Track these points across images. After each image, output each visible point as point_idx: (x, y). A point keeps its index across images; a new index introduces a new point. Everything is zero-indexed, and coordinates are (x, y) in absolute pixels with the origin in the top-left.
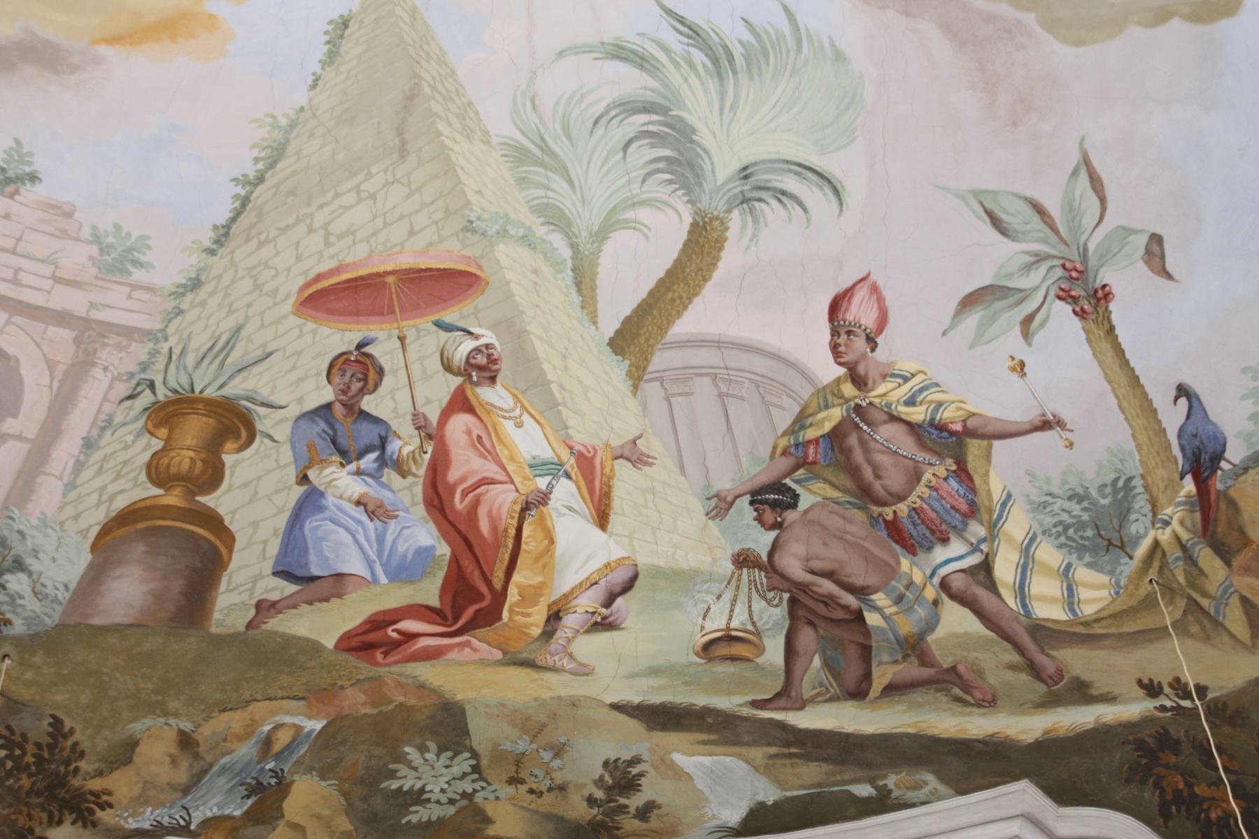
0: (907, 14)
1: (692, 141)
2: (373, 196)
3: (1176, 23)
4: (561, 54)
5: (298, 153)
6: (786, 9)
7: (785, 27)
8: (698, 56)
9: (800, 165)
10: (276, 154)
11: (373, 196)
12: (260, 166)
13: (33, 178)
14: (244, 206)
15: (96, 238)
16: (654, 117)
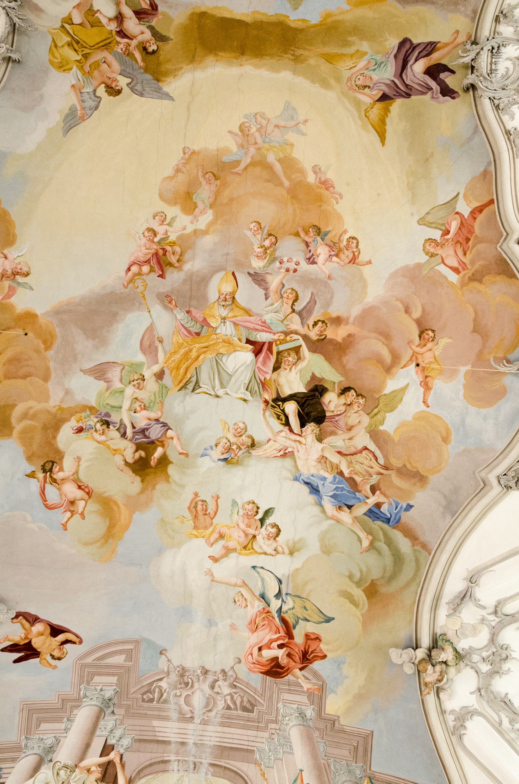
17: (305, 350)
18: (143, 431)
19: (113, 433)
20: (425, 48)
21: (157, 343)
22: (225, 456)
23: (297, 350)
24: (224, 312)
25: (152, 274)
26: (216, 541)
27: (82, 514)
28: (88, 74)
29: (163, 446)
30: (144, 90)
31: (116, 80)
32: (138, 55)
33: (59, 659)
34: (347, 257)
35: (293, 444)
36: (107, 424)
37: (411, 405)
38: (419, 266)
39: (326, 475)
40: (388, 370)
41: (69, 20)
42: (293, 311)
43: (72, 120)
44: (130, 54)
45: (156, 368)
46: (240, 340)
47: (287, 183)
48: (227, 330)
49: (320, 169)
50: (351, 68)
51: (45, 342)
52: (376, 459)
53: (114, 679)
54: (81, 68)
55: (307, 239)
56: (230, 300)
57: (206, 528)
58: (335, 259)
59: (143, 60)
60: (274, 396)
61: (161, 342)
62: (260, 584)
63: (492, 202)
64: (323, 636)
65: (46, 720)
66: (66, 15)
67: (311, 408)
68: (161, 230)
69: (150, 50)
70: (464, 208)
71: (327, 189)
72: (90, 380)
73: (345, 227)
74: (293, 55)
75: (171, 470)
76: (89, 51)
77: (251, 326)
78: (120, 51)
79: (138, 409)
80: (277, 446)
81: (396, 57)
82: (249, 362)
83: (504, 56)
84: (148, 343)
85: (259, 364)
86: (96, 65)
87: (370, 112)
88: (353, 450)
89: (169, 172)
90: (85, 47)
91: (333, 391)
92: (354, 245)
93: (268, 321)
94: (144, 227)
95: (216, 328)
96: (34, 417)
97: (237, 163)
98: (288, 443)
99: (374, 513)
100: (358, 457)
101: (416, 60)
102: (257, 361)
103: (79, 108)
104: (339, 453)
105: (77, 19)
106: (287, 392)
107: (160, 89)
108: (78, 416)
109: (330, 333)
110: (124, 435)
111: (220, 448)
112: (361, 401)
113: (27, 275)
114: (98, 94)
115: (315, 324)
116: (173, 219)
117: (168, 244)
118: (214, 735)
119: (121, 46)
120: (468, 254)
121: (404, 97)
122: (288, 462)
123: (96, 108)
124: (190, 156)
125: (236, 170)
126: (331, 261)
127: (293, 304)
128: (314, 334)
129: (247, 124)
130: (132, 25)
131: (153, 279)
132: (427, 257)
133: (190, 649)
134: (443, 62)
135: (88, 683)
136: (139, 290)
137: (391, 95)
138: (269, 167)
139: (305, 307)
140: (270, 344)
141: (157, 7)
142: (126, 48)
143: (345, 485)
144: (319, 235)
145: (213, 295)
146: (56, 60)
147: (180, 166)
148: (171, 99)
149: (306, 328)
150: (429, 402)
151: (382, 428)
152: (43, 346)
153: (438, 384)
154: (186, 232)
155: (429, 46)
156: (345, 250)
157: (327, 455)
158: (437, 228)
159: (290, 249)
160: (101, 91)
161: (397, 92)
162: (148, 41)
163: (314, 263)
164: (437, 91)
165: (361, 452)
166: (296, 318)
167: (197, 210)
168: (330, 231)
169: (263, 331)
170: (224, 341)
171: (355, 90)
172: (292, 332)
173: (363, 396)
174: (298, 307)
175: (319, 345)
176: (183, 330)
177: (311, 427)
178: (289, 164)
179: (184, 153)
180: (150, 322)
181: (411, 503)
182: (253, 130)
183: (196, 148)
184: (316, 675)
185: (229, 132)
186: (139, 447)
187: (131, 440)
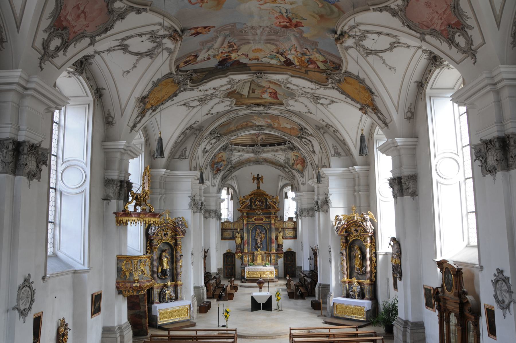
118: (264, 37)
133: (255, 22)
184: (300, 29)
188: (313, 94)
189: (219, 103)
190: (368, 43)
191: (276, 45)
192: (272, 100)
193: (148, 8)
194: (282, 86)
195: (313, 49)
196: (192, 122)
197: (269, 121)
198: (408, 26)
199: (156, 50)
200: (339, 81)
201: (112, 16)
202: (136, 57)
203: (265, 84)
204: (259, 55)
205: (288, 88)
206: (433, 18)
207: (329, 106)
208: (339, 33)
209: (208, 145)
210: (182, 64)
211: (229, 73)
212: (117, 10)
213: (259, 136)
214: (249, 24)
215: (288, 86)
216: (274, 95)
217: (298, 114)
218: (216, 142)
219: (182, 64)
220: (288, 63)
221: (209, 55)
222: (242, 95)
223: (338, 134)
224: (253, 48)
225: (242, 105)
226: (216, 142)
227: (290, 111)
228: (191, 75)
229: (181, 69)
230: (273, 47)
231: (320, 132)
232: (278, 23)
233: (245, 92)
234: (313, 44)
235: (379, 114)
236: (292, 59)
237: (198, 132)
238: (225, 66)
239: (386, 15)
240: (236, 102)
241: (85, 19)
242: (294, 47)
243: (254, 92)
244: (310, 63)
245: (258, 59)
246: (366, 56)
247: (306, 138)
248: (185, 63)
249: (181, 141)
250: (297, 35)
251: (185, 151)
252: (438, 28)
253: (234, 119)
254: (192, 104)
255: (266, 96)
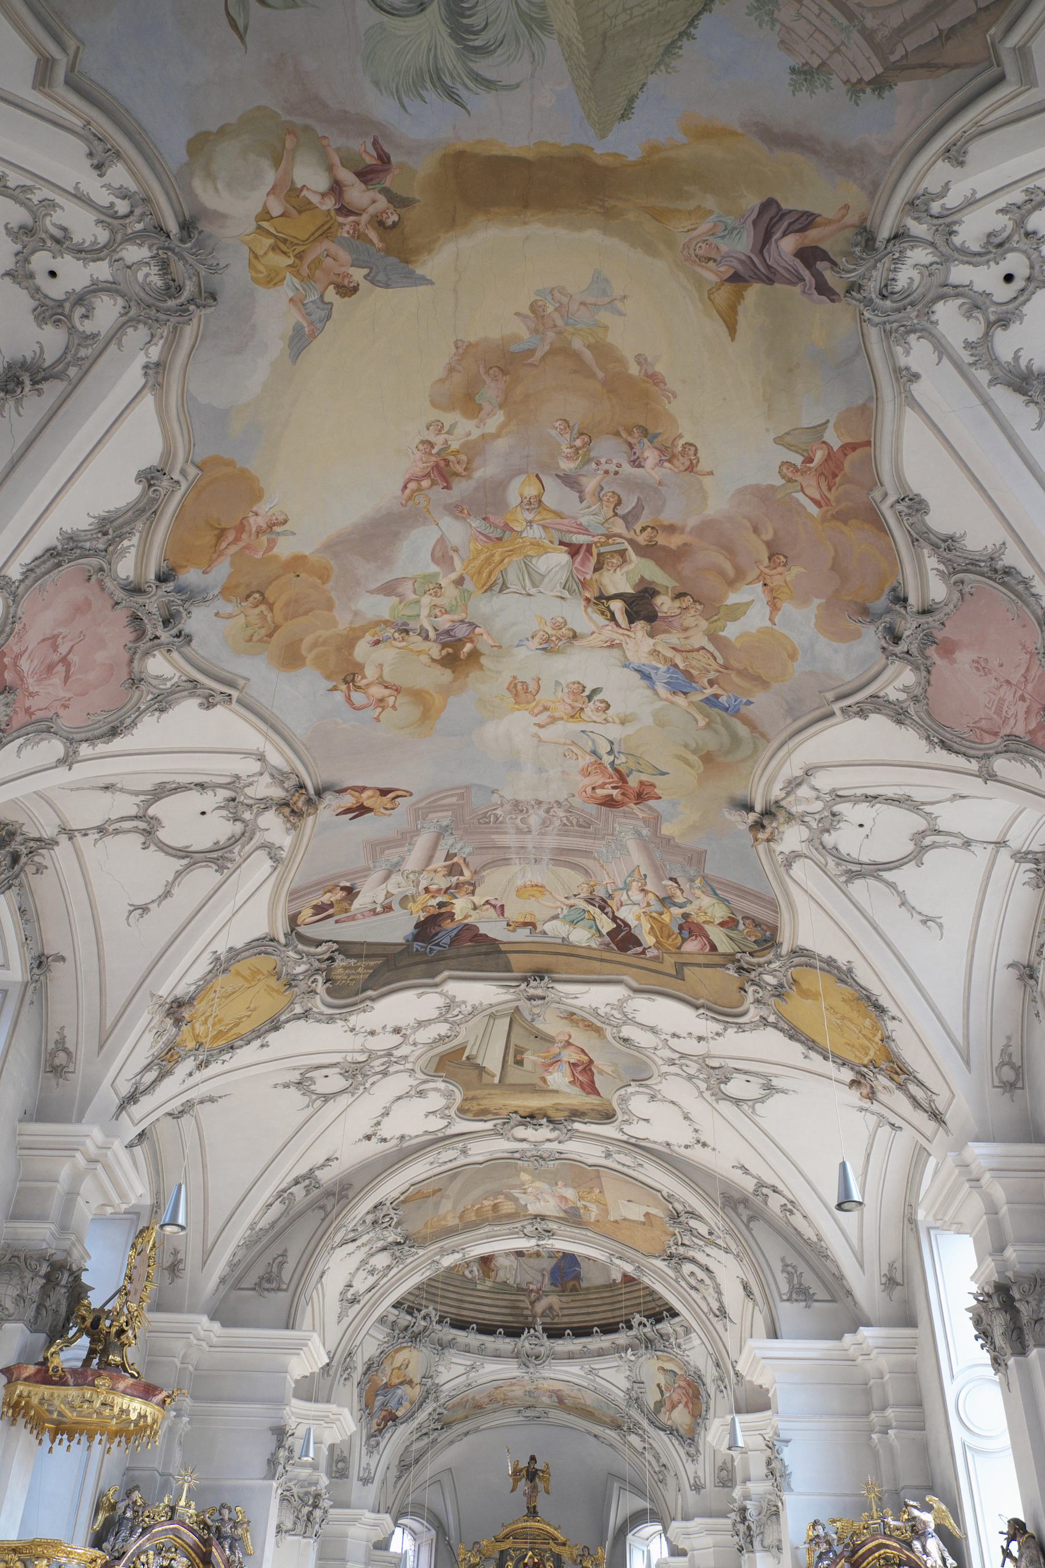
0: (345, 112)
1: (451, 28)
2: (625, 10)
3: (214, 129)
4: (518, 86)
5: (658, 47)
6: (406, 110)
7: (405, 100)
8: (448, 81)
9: (393, 14)
10: (670, 49)
11: (625, 10)
12: (679, 43)
13: (793, 70)
14: (693, 21)
15: (773, 21)
16: (471, 44)
17: (631, 553)
18: (447, 632)
19: (414, 638)
20: (798, 219)
21: (451, 553)
22: (545, 646)
23: (622, 553)
24: (530, 516)
25: (435, 487)
26: (541, 712)
27: (394, 707)
28: (309, 279)
29: (472, 641)
30: (389, 279)
31: (348, 275)
32: (373, 235)
33: (393, 809)
34: (683, 464)
35: (622, 637)
36: (407, 632)
37: (757, 618)
38: (772, 488)
39: (659, 665)
40: (732, 583)
41: (265, 215)
42: (616, 514)
43: (299, 342)
44: (360, 236)
45: (454, 576)
46: (552, 542)
47: (600, 375)
48: (536, 532)
49: (646, 360)
50: (688, 231)
51: (321, 577)
52: (715, 659)
53: (450, 813)
54: (297, 274)
55: (630, 439)
56: (537, 503)
57: (528, 703)
58: (666, 464)
59: (381, 240)
60: (597, 594)
61: (456, 550)
62: (590, 743)
63: (868, 443)
64: (657, 784)
65: (389, 848)
66: (259, 209)
67: (640, 606)
68: (439, 441)
69: (389, 222)
70: (834, 439)
71: (656, 384)
72: (380, 597)
73: (680, 431)
74: (602, 206)
75: (483, 660)
76: (302, 248)
77: (564, 528)
78: (346, 235)
79: (439, 614)
80: (602, 638)
81: (755, 223)
82: (564, 563)
83: (909, 262)
84: (440, 554)
85: (577, 565)
86: (317, 263)
87: (715, 295)
88: (689, 648)
89: (439, 372)
90: (297, 244)
91: (667, 594)
92: (692, 452)
93: (585, 523)
94: (417, 441)
95: (522, 532)
96: (324, 643)
97: (532, 352)
98: (615, 636)
99: (712, 701)
100: (695, 654)
101: (784, 234)
102: (573, 563)
103: (305, 325)
104: (673, 648)
105: (276, 210)
106: (612, 591)
107: (412, 272)
108: (372, 631)
109: (661, 539)
110: (427, 638)
111: (537, 640)
112: (699, 607)
113: (285, 522)
114: (327, 299)
115: (643, 529)
116: (453, 426)
117: (449, 454)
118: (551, 841)
119: (347, 228)
120: (834, 489)
121: (764, 282)
122: (616, 652)
123: (329, 317)
124: (464, 350)
125: (530, 361)
126: (662, 466)
127: (615, 508)
128: (642, 539)
129: (540, 303)
130: (357, 194)
131: (438, 493)
132: (783, 482)
133: (522, 786)
134: (824, 246)
135: (424, 819)
136: (421, 506)
137: (747, 277)
138: (576, 355)
139: (630, 512)
140: (589, 547)
141: (389, 158)
142: (354, 229)
143: (680, 676)
144: (645, 437)
145: (513, 497)
146: (261, 275)
147: (453, 364)
148: (430, 282)
149: (632, 532)
150: (776, 621)
151: (721, 634)
152: (319, 581)
153: (787, 607)
154: (469, 438)
155: (805, 217)
156: (681, 458)
157: (659, 648)
158: (797, 452)
159: (609, 451)
160: (331, 294)
161: (755, 274)
162: (384, 212)
163: (640, 466)
164: (811, 286)
165: (698, 650)
166: (620, 522)
167: (482, 413)
168: (659, 434)
169: (579, 533)
170: (532, 544)
171: (695, 262)
172: (615, 535)
173: (701, 603)
174: (622, 511)
175: (647, 551)
176: (481, 537)
177: (640, 625)
178: (603, 351)
179: (457, 348)
180: (440, 533)
181: (751, 699)
182: (550, 309)
183: (472, 339)
184: (650, 808)
185: (516, 314)
186: (444, 645)
187: (435, 641)
188: (705, 1057)
189: (408, 1095)
190: (846, 840)
191: (586, 872)
192: (577, 1098)
193: (235, 694)
194: (609, 1031)
195: (692, 881)
196: (317, 1157)
197: (570, 1193)
198: (944, 745)
199: (237, 849)
200: (779, 992)
201: (137, 693)
202: (179, 864)
203: (551, 1025)
204: (537, 909)
205: (626, 1040)
206: (1002, 701)
207: (758, 1106)
208: (758, 808)
209: (362, 1274)
210: (306, 915)
211: (446, 973)
212: (154, 682)
213: (538, 1299)
214: (508, 794)
215: (627, 1031)
216: (585, 1074)
217: (664, 1157)
218: (389, 1268)
219: (306, 915)
220: (623, 938)
221: (389, 895)
222: (481, 1069)
223: (797, 1220)
224: (519, 882)
225: (482, 1114)
226: (389, 1268)
227: (637, 1146)
228: (331, 959)
229: (302, 930)
230: (575, 880)
231: (739, 1215)
232: (589, 790)
233: (492, 1060)
234: (691, 859)
235: (913, 1088)
236: (632, 922)
237: (329, 1203)
238: (438, 946)
239: (879, 723)
240: (465, 1100)
241: (66, 682)
242: (636, 876)
243: (519, 1063)
244: (686, 933)
245: (532, 925)
246: (846, 882)
247: (693, 1261)
248: (319, 909)
249: (273, 1225)
250: (645, 832)
251: (282, 1263)
252: (1020, 730)
253: (454, 1174)
254: (324, 1085)
255: (559, 1079)
